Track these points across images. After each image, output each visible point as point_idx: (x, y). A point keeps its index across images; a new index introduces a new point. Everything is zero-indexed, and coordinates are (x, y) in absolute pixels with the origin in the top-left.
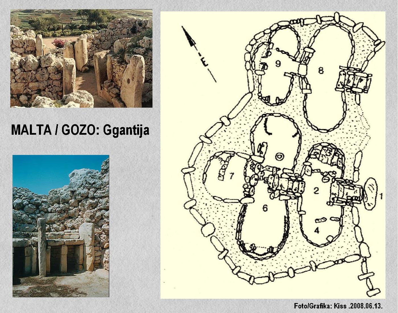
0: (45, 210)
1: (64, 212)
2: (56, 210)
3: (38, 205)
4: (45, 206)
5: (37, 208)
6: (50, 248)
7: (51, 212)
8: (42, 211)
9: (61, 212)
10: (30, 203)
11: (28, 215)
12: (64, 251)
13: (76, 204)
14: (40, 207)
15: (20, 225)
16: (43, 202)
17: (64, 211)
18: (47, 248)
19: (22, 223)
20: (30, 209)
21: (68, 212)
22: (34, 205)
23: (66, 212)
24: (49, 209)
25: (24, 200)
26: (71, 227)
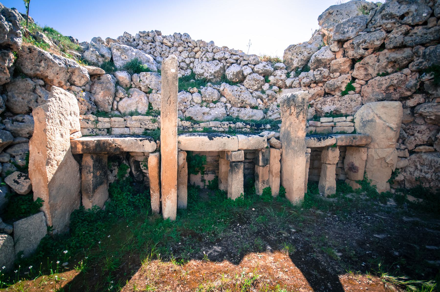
1: (315, 85)
3: (266, 75)
4: (281, 76)
5: (267, 81)
6: (310, 152)
7: (291, 87)
8: (274, 84)
9: (309, 86)
10: (253, 72)
11: (251, 93)
13: (346, 67)
14: (271, 78)
15: (238, 111)
19: (241, 107)
22: (260, 74)
23: (321, 84)
24: (288, 82)
26: (331, 112)
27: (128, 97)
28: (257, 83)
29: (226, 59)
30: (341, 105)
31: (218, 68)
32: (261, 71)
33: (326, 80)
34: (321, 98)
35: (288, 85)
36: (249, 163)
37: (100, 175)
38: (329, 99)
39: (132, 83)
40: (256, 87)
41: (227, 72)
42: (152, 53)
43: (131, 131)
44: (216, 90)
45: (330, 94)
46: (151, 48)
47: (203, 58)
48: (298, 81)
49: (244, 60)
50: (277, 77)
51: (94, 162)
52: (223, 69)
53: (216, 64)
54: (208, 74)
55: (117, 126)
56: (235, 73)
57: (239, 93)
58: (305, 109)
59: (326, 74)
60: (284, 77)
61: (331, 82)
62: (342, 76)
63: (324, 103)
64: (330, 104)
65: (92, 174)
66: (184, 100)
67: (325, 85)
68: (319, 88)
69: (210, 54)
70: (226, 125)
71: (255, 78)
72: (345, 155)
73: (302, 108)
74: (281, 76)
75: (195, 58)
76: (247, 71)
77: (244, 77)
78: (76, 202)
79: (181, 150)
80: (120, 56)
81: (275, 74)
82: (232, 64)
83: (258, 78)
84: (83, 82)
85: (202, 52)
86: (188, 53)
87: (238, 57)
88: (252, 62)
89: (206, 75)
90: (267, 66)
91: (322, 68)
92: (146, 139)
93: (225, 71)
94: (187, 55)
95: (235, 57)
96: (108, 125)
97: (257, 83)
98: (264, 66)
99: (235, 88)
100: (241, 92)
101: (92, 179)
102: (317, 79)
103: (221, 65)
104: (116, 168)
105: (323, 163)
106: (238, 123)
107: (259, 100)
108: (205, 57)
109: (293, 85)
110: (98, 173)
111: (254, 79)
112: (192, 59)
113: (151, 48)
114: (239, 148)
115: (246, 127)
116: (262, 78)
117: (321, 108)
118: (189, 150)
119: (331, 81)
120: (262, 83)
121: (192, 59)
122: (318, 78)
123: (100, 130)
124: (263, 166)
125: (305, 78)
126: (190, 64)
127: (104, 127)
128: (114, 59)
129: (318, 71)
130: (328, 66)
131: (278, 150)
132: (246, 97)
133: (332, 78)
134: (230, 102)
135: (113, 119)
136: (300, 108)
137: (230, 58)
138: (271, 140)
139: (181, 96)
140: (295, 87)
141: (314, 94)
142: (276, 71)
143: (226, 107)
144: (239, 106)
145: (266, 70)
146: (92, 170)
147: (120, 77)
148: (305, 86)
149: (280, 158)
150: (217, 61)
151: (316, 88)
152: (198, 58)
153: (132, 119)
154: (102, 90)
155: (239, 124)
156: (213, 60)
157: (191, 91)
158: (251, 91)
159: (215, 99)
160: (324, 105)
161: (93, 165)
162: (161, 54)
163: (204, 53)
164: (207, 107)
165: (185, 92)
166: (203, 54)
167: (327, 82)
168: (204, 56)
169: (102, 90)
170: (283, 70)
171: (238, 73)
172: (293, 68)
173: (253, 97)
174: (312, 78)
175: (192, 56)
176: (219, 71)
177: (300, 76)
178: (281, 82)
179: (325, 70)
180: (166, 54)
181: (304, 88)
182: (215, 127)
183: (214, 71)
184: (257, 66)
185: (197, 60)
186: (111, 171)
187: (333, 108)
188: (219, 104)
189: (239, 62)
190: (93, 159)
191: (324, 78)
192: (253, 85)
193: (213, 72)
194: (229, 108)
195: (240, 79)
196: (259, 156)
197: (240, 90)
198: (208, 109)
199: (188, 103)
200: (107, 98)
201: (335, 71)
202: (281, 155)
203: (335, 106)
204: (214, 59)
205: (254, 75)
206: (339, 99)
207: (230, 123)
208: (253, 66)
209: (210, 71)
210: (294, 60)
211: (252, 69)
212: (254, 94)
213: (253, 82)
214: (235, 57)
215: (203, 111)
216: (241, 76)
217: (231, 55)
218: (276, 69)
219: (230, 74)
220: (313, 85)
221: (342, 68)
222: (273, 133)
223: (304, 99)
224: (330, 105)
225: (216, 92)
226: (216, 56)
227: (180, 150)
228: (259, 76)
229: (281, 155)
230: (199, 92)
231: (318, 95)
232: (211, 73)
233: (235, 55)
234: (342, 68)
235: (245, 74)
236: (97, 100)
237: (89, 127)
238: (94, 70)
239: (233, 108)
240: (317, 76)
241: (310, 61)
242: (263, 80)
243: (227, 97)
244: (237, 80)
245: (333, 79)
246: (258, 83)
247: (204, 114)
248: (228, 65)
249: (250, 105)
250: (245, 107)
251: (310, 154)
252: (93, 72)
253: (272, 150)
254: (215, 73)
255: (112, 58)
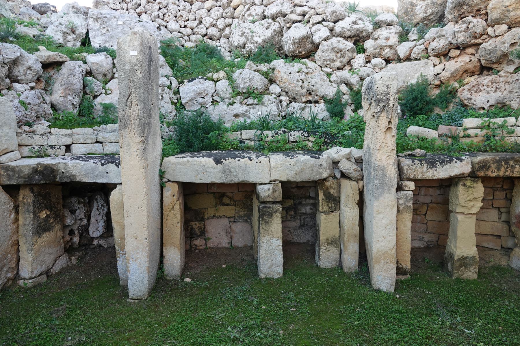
0: (388, 53)
1: (458, 52)
2: (426, 49)
3: (358, 40)
4: (387, 39)
7: (408, 59)
11: (329, 75)
12: (469, 200)
14: (369, 44)
16: (378, 25)
17: (462, 48)
18: (399, 188)
19: (310, 102)
20: (334, 54)
21: (477, 50)
22: (347, 38)
23: (470, 50)
24: (403, 50)
25: (313, 25)
27: (106, 94)
28: (339, 55)
29: (284, 15)
30: (510, 92)
31: (268, 33)
32: (348, 34)
33: (480, 41)
34: (472, 79)
35: (402, 56)
36: (312, 204)
37: (48, 216)
38: (486, 79)
39: (115, 70)
40: (338, 64)
41: (284, 39)
42: (161, 17)
43: (106, 148)
44: (258, 74)
45: (491, 69)
46: (160, 9)
47: (246, 15)
48: (422, 47)
49: (317, 14)
50: (381, 42)
51: (35, 196)
52: (280, 33)
53: (266, 25)
54: (252, 45)
55: (81, 141)
56: (296, 41)
57: (302, 77)
58: (391, 105)
59: (479, 30)
60: (394, 39)
61: (490, 45)
62: (513, 30)
63: (476, 89)
64: (489, 89)
65: (32, 216)
66: (201, 93)
67: (479, 51)
68: (466, 58)
69: (257, 8)
70: (270, 136)
71: (335, 45)
72: (512, 196)
73: (383, 104)
74: (387, 39)
75: (234, 18)
76: (321, 33)
77: (317, 47)
78: (9, 255)
79: (169, 181)
80: (98, 30)
81: (376, 36)
82: (294, 22)
83: (341, 46)
84: (30, 75)
85: (245, 6)
86: (221, 10)
87: (306, 9)
88: (329, 17)
89: (250, 46)
90: (360, 22)
91: (470, 18)
92: (112, 163)
93: (282, 36)
94: (219, 13)
95: (299, 10)
96: (67, 141)
97: (339, 55)
98: (354, 23)
99: (297, 66)
100: (307, 73)
101: (32, 222)
102: (460, 40)
103: (275, 26)
104: (82, 205)
105: (452, 212)
106: (293, 133)
107: (344, 88)
108: (250, 15)
109: (413, 56)
110: (43, 215)
111: (333, 49)
112: (228, 21)
113: (160, 9)
114: (272, 179)
115: (309, 140)
116: (350, 45)
117: (471, 99)
118: (181, 180)
119: (489, 43)
120: (350, 54)
121: (228, 21)
122: (461, 38)
123: (52, 147)
124: (327, 213)
125: (437, 40)
126: (223, 30)
127: (60, 143)
128: (90, 35)
129: (462, 24)
130: (484, 12)
131: (354, 183)
132: (316, 83)
133: (491, 37)
134: (287, 92)
135: (75, 130)
136: (381, 105)
137: (292, 12)
138: (339, 165)
139: (195, 88)
140: (416, 59)
141: (456, 71)
142: (379, 30)
143: (281, 101)
144: (304, 100)
145: (357, 30)
146: (31, 209)
147: (93, 63)
148: (437, 56)
149: (357, 198)
150: (270, 20)
151: (460, 59)
152: (238, 18)
153: (106, 129)
154: (61, 86)
155: (294, 135)
156: (263, 19)
157: (215, 76)
158: (329, 70)
159: (257, 89)
160: (476, 91)
161: (33, 201)
162: (176, 17)
163: (247, 7)
164: (241, 103)
165: (202, 80)
166: (245, 10)
167: (481, 46)
168: (248, 13)
169: (61, 86)
170: (391, 27)
171: (304, 38)
172: (416, 21)
173: (330, 81)
174: (450, 39)
175: (228, 14)
176: (272, 38)
177: (427, 36)
178: (388, 50)
179: (475, 20)
180: (184, 16)
181: (436, 60)
182: (249, 139)
183: (263, 38)
184: (340, 23)
185: (236, 20)
186: (73, 212)
187: (493, 97)
188: (266, 97)
189: (307, 16)
190: (32, 192)
191: (475, 38)
192: (333, 61)
193: (260, 41)
194: (284, 104)
195: (307, 51)
196: (317, 195)
197: (306, 71)
198: (244, 108)
199: (208, 99)
200: (70, 97)
201: (498, 22)
202: (361, 193)
203: (499, 94)
204: (264, 17)
205: (334, 40)
206: (509, 79)
207: (276, 134)
208: (331, 24)
209: (256, 39)
210: (417, 6)
211: (331, 30)
212: (333, 78)
213: (332, 55)
214: (299, 10)
215: (235, 112)
216: (309, 46)
217: (294, 6)
218: (378, 25)
219: (289, 42)
220: (454, 53)
221: (512, 14)
222: (346, 150)
223: (388, 87)
224: (488, 93)
225: (258, 77)
226: (267, 11)
227: (165, 180)
228: (344, 41)
229: (361, 193)
230: (229, 78)
231: (465, 71)
232: (257, 42)
233: (300, 6)
234: (512, 14)
235: (316, 39)
236: (55, 102)
237: (33, 143)
238: (49, 57)
239: (293, 103)
240: (460, 35)
241: (447, 5)
242: (352, 48)
243: (281, 86)
244: (303, 53)
245: (494, 39)
246: (343, 56)
247: (236, 116)
248: (288, 25)
249: (323, 98)
250: (316, 102)
251: (411, 193)
252: (47, 59)
253: (345, 183)
254: (264, 41)
255: (87, 33)
